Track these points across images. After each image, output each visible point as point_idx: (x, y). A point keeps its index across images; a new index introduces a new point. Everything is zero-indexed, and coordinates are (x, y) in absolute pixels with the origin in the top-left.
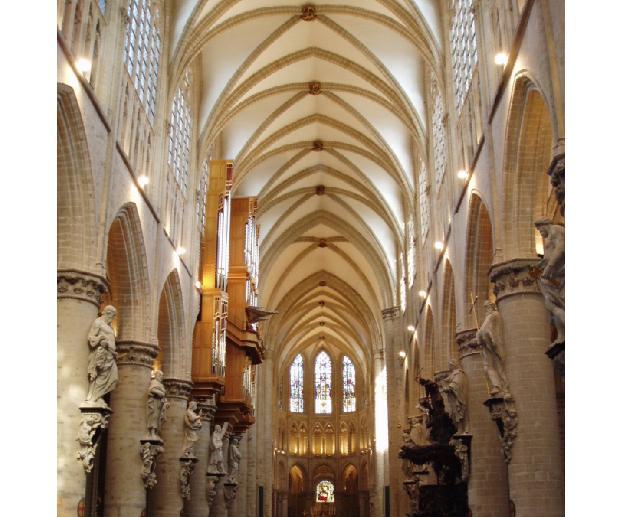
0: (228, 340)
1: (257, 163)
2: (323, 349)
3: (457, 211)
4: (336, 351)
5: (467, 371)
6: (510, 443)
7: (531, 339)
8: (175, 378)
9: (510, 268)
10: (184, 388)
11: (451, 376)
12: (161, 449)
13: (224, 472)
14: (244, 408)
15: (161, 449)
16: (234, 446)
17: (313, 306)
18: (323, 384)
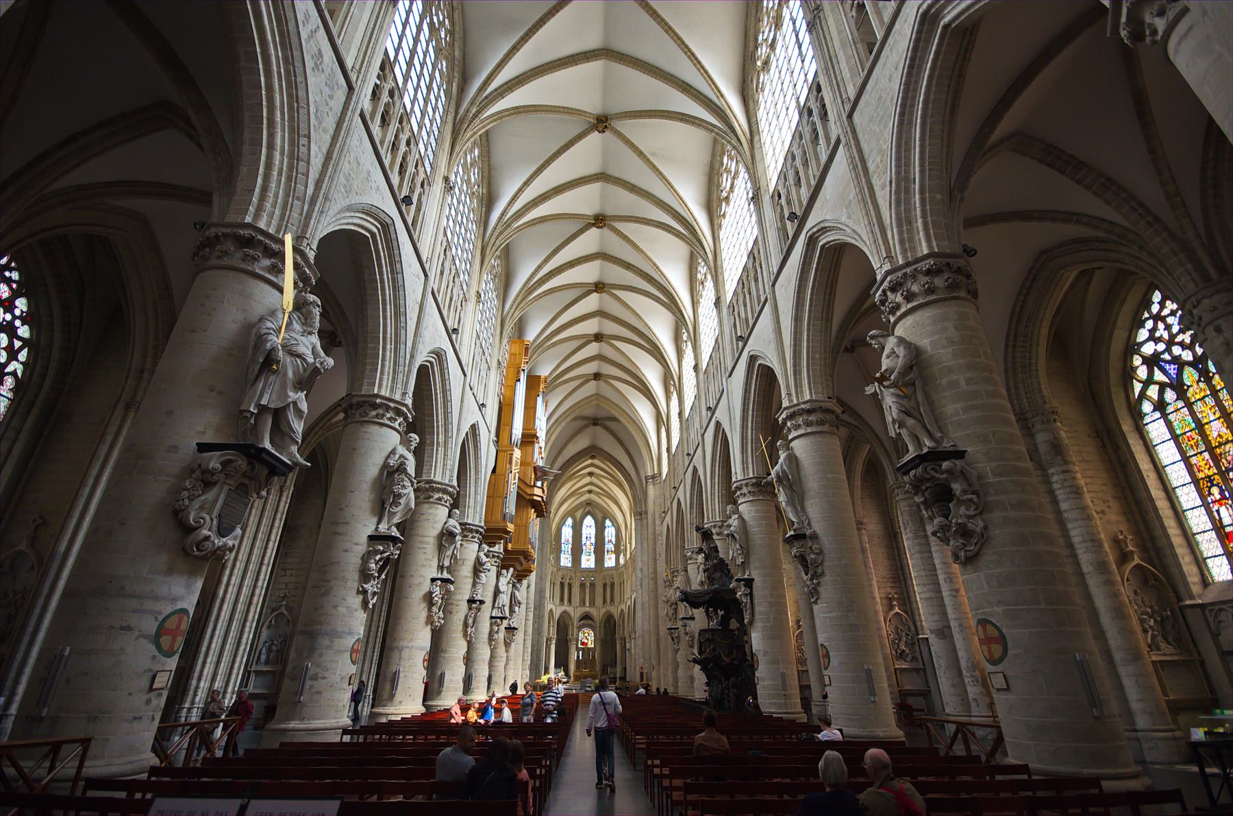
0: (518, 494)
1: (549, 348)
2: (589, 513)
3: (730, 376)
4: (599, 515)
5: (746, 517)
6: (815, 581)
7: (829, 476)
8: (469, 522)
9: (802, 409)
10: (477, 532)
11: (730, 521)
12: (452, 587)
13: (508, 615)
14: (527, 556)
15: (452, 587)
16: (516, 592)
17: (583, 476)
18: (588, 543)
